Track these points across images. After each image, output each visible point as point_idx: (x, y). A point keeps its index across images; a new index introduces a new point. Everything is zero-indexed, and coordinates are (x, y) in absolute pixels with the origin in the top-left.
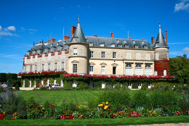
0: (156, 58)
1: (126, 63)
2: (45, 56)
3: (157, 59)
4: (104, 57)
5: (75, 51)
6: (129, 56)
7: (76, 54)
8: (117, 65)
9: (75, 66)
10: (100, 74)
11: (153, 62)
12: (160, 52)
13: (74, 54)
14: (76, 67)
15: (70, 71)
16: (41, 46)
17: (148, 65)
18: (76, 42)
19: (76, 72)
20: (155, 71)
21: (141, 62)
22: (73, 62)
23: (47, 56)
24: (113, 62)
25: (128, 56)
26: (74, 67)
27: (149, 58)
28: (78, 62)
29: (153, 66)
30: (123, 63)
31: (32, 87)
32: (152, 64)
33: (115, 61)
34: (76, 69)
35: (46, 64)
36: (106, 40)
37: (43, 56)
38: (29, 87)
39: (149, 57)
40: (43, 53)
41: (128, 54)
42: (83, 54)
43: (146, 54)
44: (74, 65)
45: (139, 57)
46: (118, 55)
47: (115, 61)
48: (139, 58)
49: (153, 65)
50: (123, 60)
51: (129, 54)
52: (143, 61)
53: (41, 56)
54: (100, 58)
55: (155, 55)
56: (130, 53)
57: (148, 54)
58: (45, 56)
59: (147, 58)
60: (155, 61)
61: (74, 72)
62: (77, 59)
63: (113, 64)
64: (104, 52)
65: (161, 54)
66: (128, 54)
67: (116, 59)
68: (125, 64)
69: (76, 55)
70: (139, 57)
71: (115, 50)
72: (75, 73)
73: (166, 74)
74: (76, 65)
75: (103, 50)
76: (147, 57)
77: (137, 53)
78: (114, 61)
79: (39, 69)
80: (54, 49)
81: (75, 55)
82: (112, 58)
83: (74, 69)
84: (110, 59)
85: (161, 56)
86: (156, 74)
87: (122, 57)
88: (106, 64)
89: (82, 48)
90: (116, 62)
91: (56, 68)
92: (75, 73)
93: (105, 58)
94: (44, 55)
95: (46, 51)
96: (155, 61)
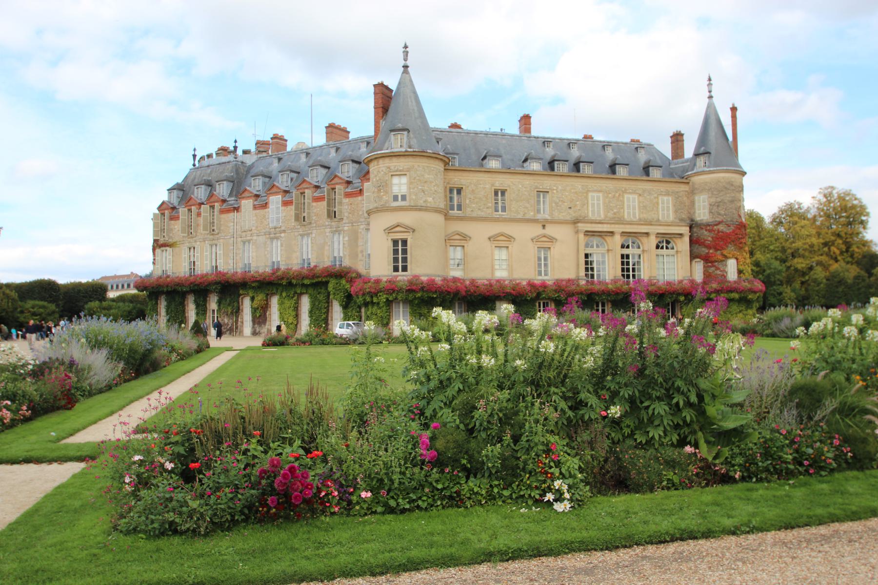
0: (697, 212)
1: (588, 233)
2: (255, 207)
3: (702, 214)
4: (504, 209)
5: (400, 185)
6: (598, 205)
7: (404, 198)
8: (552, 240)
9: (400, 251)
10: (489, 277)
11: (685, 230)
12: (713, 190)
13: (396, 198)
14: (405, 252)
15: (378, 266)
16: (229, 166)
17: (665, 242)
18: (404, 150)
19: (405, 269)
20: (691, 261)
21: (644, 229)
22: (390, 230)
23: (265, 206)
24: (537, 230)
25: (593, 205)
26: (396, 252)
27: (668, 216)
28: (414, 231)
29: (683, 245)
30: (577, 232)
31: (255, 333)
33: (544, 226)
34: (405, 260)
35: (262, 239)
36: (504, 142)
37: (243, 209)
38: (241, 332)
39: (668, 211)
40: (246, 194)
41: (593, 197)
43: (660, 198)
44: (395, 242)
45: (634, 208)
46: (556, 203)
47: (544, 226)
48: (634, 214)
49: (687, 239)
50: (575, 222)
51: (598, 200)
52: (650, 223)
53: (237, 209)
54: (489, 212)
55: (693, 203)
56: (601, 194)
57: (665, 198)
58: (255, 207)
59: (663, 214)
60: (693, 225)
61: (396, 269)
62: (407, 218)
64: (503, 193)
65: (719, 200)
66: (593, 197)
67: (547, 217)
68: (581, 236)
69: (403, 203)
70: (634, 208)
71: (547, 183)
72: (402, 277)
73: (736, 274)
74: (405, 242)
75: (501, 181)
76: (663, 210)
77: (626, 196)
78: (541, 227)
79: (231, 262)
80: (292, 179)
81: (400, 203)
82: (531, 214)
83: (396, 260)
84: (527, 216)
85: (718, 204)
86: (698, 272)
87: (570, 211)
88: (510, 238)
89: (427, 176)
90: (551, 230)
91: (305, 257)
92: (400, 273)
93: (505, 215)
94: (247, 204)
95: (256, 185)
96: (693, 225)
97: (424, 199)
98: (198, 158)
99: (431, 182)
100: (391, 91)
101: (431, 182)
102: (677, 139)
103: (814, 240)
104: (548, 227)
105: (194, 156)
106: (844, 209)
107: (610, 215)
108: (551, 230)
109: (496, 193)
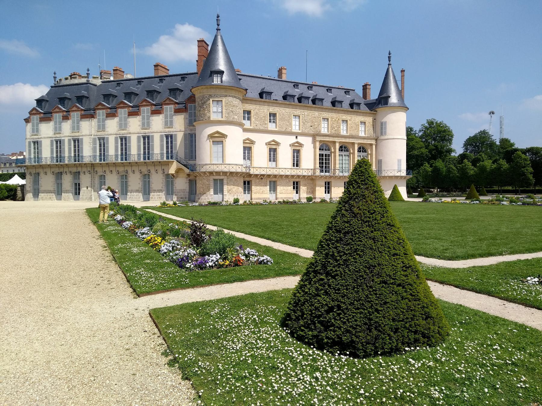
8: (301, 145)
21: (351, 141)
24: (293, 139)
32: (371, 145)
42: (236, 117)
63: (292, 145)
90: (301, 139)
97: (233, 117)
98: (57, 79)
99: (237, 106)
100: (208, 45)
101: (237, 106)
102: (365, 88)
103: (424, 150)
104: (298, 137)
105: (55, 78)
106: (440, 132)
107: (333, 131)
108: (301, 139)
109: (270, 116)
